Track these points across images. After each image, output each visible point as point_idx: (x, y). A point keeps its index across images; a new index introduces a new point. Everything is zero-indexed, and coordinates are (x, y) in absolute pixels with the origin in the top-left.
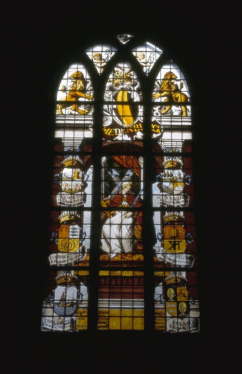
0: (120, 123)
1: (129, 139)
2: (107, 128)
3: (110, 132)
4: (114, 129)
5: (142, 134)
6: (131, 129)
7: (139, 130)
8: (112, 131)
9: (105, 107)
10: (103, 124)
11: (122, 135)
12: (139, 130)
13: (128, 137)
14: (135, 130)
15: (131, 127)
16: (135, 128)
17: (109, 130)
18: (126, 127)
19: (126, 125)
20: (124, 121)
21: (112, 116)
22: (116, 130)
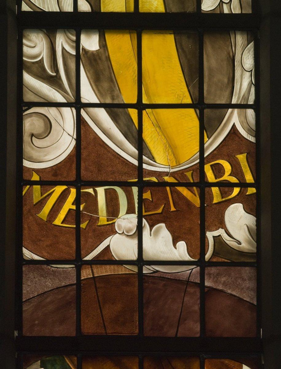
0: (127, 152)
1: (181, 251)
2: (51, 177)
3: (69, 205)
4: (91, 191)
5: (250, 220)
6: (188, 185)
7: (236, 191)
8: (77, 202)
9: (35, 46)
10: (20, 155)
11: (140, 228)
12: (236, 191)
13: (175, 243)
14: (215, 190)
15: (189, 174)
16: (214, 185)
17: (64, 196)
18: (159, 174)
19: (160, 163)
20: (150, 135)
21: (77, 104)
22: (101, 191)
